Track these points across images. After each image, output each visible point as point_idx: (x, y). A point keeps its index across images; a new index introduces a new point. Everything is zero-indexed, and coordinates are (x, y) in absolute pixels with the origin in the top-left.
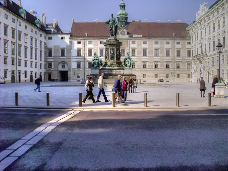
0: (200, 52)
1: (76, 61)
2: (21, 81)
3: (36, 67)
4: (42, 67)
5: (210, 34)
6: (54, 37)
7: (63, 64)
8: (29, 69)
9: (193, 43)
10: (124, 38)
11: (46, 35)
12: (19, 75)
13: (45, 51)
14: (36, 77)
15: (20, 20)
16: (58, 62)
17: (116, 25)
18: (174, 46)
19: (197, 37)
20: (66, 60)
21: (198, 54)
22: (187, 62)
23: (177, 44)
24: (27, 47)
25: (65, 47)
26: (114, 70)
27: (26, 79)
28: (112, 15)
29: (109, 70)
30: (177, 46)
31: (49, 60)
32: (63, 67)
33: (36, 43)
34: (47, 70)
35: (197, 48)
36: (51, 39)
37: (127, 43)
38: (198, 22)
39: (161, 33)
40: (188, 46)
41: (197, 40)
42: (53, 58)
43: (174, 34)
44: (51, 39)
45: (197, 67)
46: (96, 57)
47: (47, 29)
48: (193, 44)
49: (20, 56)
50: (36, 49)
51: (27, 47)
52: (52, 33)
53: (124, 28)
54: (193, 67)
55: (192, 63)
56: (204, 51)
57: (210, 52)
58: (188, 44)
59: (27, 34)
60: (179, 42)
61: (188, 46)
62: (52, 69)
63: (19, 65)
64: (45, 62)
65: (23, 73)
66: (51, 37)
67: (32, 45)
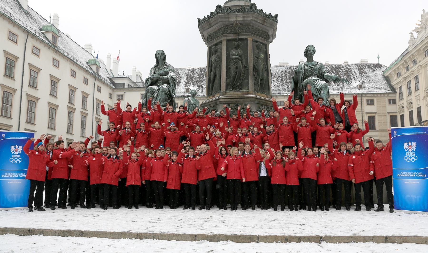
9: (401, 99)
11: (113, 91)
19: (417, 83)
41: (417, 89)
46: (162, 72)
48: (402, 102)
58: (390, 103)
59: (58, 77)
60: (372, 101)
61: (391, 108)
66: (122, 96)
67: (73, 104)
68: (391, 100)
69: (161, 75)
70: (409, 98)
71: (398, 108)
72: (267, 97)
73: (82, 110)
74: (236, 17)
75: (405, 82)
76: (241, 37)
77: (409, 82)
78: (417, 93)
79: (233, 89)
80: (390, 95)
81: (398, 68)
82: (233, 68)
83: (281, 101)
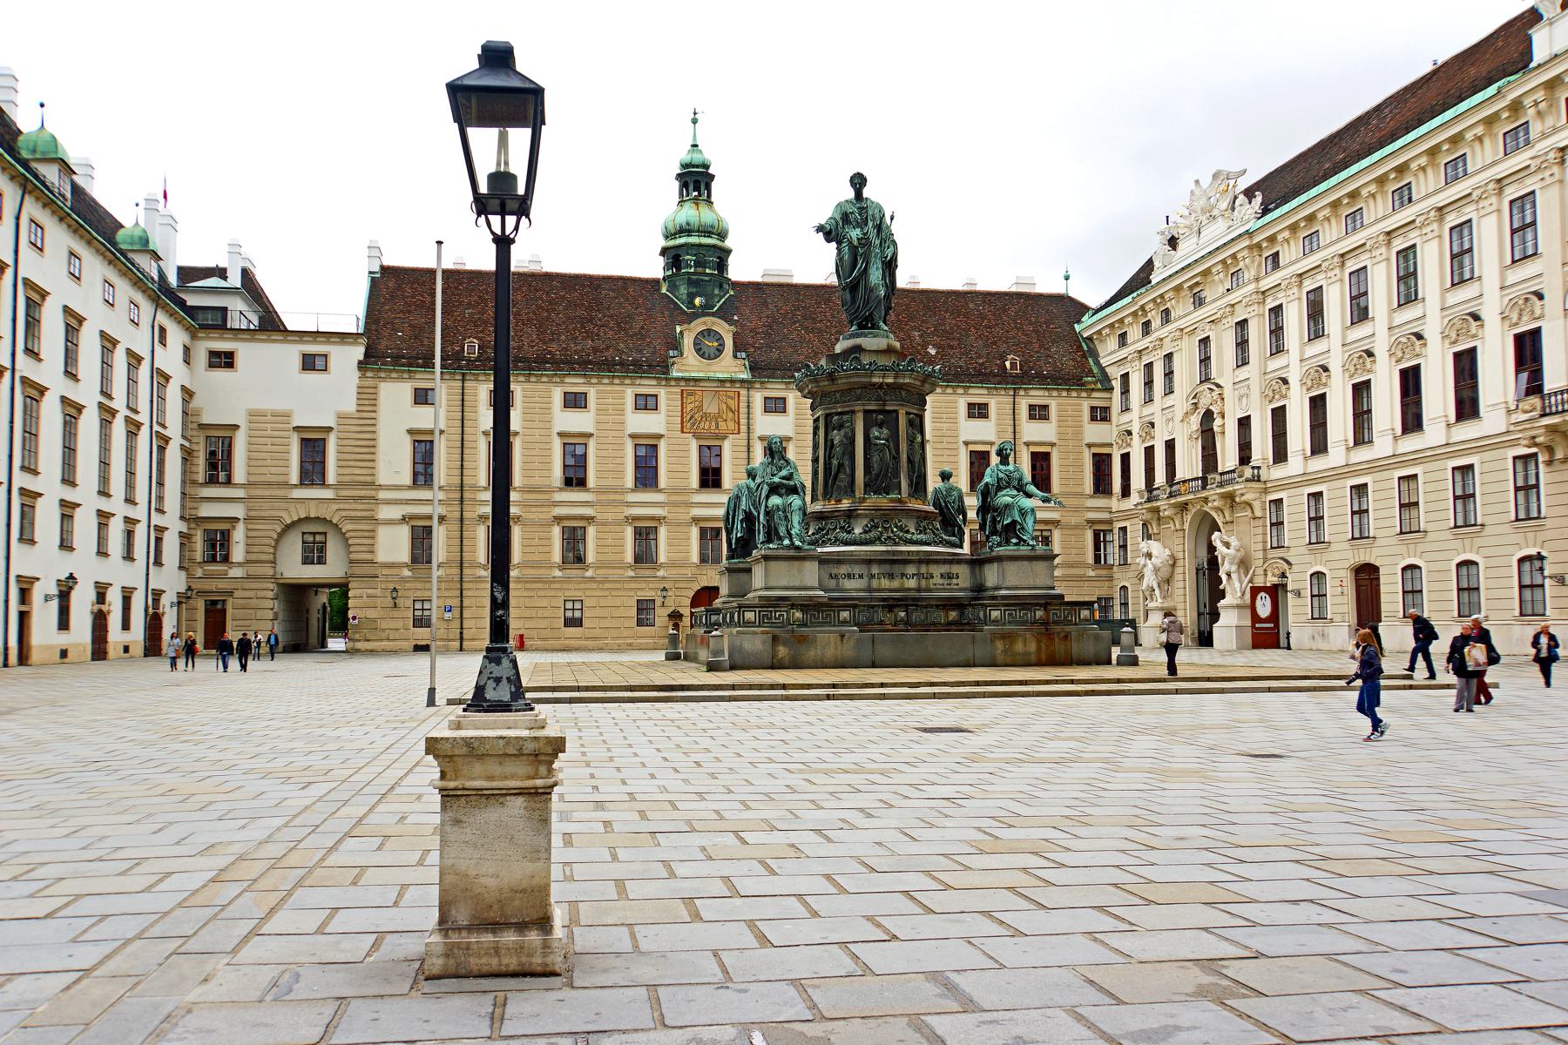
0: (1189, 464)
1: (404, 519)
2: (35, 656)
3: (129, 556)
4: (165, 559)
5: (1278, 349)
6: (245, 352)
7: (314, 534)
8: (87, 568)
10: (720, 375)
12: (24, 608)
13: (187, 444)
14: (126, 625)
15: (32, 208)
16: (279, 519)
17: (889, 253)
18: (1015, 432)
19: (1169, 374)
20: (335, 507)
21: (1179, 476)
22: (1091, 522)
23: (1032, 417)
24: (80, 409)
25: (331, 422)
26: (911, 569)
27: (63, 639)
28: (858, 181)
29: (875, 570)
30: (1035, 432)
31: (206, 511)
32: (314, 553)
33: (132, 381)
34: (199, 573)
35: (1170, 446)
36: (230, 365)
37: (732, 403)
38: (1178, 289)
39: (932, 351)
40: (1095, 433)
41: (1169, 390)
42: (240, 493)
43: (1013, 365)
44: (230, 365)
45: (1180, 555)
46: (784, 473)
47: (192, 301)
48: (1126, 417)
49: (35, 472)
50: (132, 428)
51: (80, 409)
52: (234, 322)
53: (713, 315)
54: (1149, 555)
55: (1124, 529)
56: (1228, 456)
57: (1280, 455)
58: (1093, 419)
60: (1045, 407)
61: (1095, 433)
62: (236, 572)
63: (21, 540)
64: (182, 518)
65: (47, 598)
68: (1097, 408)
69: (783, 478)
70: (1148, 410)
71: (1115, 433)
72: (924, 504)
73: (129, 413)
74: (883, 377)
75: (1137, 363)
76: (888, 408)
77: (1149, 366)
78: (1169, 401)
79: (875, 493)
80: (1095, 395)
81: (1121, 321)
82: (876, 458)
83: (776, 398)
